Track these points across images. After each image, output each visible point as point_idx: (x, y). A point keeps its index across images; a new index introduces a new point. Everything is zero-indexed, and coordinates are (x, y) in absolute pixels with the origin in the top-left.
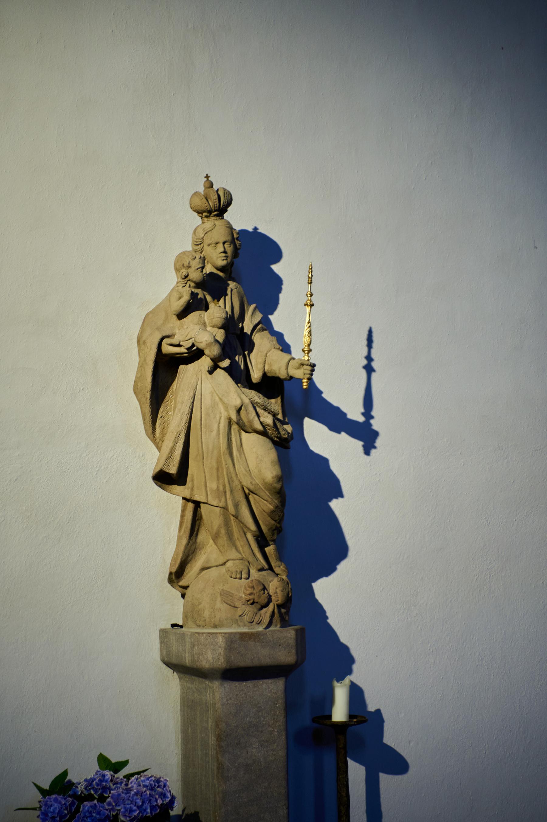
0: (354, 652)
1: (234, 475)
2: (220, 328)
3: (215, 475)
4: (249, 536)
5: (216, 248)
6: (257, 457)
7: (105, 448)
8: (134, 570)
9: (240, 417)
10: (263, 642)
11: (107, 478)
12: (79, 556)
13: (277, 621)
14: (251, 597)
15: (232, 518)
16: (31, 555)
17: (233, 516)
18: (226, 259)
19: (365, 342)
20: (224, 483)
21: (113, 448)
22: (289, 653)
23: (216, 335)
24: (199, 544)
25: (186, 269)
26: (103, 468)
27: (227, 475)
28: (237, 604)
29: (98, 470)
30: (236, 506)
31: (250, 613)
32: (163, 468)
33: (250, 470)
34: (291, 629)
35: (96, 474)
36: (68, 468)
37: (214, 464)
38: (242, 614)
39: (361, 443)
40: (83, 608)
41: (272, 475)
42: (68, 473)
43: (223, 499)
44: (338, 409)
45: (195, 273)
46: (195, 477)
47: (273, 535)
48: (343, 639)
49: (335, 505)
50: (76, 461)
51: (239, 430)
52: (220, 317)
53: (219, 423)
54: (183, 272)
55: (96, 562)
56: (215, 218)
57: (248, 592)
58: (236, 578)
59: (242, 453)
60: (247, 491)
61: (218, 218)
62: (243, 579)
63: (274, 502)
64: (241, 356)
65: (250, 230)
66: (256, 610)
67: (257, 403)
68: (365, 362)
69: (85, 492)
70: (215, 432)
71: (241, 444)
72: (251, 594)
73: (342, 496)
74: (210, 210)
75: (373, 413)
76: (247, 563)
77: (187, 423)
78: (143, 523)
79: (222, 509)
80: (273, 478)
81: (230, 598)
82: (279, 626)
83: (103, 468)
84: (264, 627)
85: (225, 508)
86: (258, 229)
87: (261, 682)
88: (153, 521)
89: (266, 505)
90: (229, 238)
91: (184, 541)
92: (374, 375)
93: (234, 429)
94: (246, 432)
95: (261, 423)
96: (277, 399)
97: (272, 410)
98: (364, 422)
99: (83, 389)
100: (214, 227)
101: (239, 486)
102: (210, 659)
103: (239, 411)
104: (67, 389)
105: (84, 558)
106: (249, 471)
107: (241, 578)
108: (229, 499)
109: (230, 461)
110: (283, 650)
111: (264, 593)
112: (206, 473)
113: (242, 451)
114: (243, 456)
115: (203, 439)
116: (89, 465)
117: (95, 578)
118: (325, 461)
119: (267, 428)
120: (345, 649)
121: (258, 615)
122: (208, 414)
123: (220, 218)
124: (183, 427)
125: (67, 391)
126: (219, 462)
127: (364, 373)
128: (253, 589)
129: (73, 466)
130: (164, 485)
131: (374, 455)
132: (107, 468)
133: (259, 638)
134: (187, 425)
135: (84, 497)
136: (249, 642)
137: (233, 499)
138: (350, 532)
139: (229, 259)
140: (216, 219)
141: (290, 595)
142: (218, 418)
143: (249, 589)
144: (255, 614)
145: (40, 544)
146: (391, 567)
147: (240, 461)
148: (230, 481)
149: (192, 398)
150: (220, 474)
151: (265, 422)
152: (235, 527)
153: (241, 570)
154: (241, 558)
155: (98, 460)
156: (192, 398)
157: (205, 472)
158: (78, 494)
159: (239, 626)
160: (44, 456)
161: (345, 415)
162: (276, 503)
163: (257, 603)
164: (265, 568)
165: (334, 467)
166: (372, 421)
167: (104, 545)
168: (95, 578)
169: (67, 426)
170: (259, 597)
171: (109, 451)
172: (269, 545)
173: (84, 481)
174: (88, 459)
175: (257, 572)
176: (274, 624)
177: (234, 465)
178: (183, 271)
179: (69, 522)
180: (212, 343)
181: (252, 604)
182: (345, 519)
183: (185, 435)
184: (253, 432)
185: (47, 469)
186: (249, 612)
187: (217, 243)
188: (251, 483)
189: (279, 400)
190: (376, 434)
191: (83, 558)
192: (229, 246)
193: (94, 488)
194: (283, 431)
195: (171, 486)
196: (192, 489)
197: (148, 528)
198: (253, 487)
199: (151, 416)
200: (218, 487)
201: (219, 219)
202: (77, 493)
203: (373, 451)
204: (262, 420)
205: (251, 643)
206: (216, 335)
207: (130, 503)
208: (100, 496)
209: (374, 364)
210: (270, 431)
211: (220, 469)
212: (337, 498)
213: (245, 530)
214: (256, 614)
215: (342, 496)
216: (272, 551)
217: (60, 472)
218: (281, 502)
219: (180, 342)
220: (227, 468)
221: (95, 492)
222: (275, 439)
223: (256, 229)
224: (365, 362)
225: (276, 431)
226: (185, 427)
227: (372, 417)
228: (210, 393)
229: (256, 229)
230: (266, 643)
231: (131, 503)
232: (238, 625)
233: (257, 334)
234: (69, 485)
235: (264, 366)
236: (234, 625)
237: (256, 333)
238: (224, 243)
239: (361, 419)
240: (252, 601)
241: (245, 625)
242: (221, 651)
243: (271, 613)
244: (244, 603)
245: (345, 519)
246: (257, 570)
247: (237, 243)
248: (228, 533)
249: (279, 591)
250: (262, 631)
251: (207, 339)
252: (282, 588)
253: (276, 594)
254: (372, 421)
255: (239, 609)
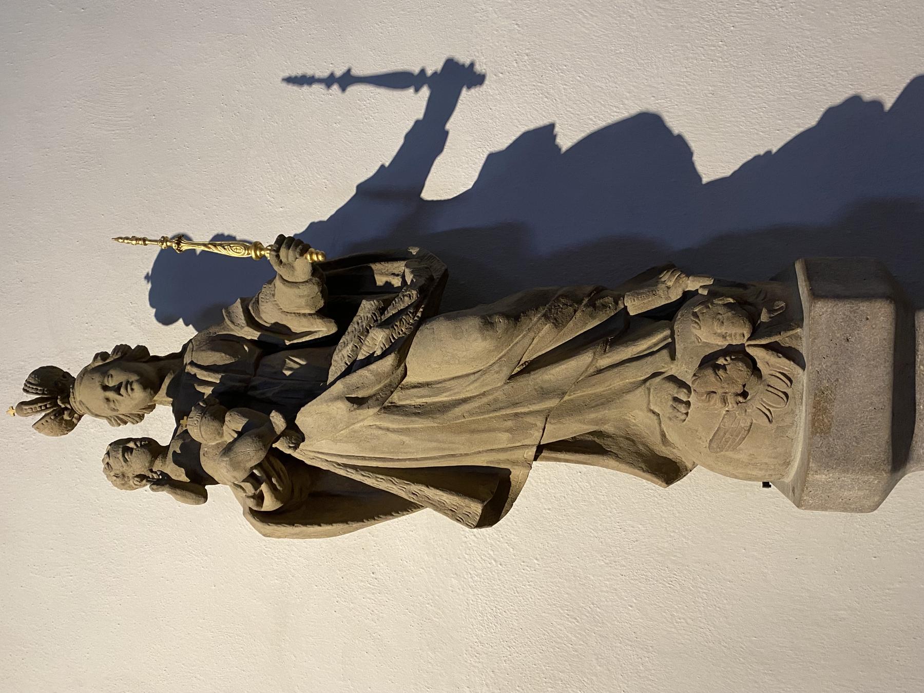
0: (838, 99)
1: (485, 400)
2: (222, 421)
3: (485, 436)
4: (604, 362)
5: (117, 400)
6: (448, 362)
7: (462, 546)
8: (661, 513)
9: (370, 397)
10: (837, 380)
11: (508, 547)
12: (631, 606)
13: (787, 335)
14: (731, 399)
15: (566, 398)
16: (626, 688)
17: (562, 398)
18: (131, 384)
19: (305, 88)
20: (498, 417)
21: (462, 533)
22: (868, 319)
23: (234, 430)
24: (619, 428)
25: (129, 481)
26: (491, 553)
27: (483, 413)
28: (744, 424)
29: (495, 561)
30: (544, 393)
31: (764, 399)
32: (472, 526)
33: (474, 373)
34: (810, 311)
35: (501, 564)
36: (490, 611)
37: (464, 437)
38: (766, 415)
39: (464, 91)
40: (719, 608)
41: (480, 340)
42: (498, 611)
43: (530, 419)
44: (407, 137)
45: (133, 465)
46: (492, 459)
47: (605, 306)
48: (812, 121)
49: (566, 140)
50: (480, 596)
51: (401, 388)
52: (199, 428)
53: (388, 429)
54: (135, 484)
55: (643, 578)
56: (71, 400)
57: (719, 405)
58: (687, 414)
59: (443, 385)
60: (518, 369)
61: (71, 394)
62: (689, 400)
63: (535, 325)
64: (287, 361)
65: (149, 286)
66: (761, 387)
67: (356, 349)
68: (335, 87)
69: (528, 587)
70: (405, 439)
71: (428, 384)
72: (724, 401)
73: (552, 126)
74: (55, 415)
75: (416, 70)
76: (658, 379)
77: (393, 481)
78: (581, 492)
79: (548, 419)
80: (485, 339)
81: (727, 435)
82: (799, 330)
83: (491, 553)
84: (800, 370)
85: (547, 415)
86: (148, 274)
87: (922, 367)
88: (579, 474)
89: (543, 337)
90: (97, 378)
91: (612, 462)
92: (356, 72)
93: (399, 400)
94: (405, 375)
95: (384, 355)
96: (375, 272)
97: (369, 316)
98: (430, 87)
99: (373, 573)
100: (83, 404)
101: (506, 387)
102: (861, 493)
103: (358, 402)
104: (373, 598)
105: (636, 599)
106: (476, 375)
107: (688, 404)
108: (529, 408)
109: (458, 411)
110: (858, 334)
111: (724, 367)
112: (481, 450)
113: (439, 385)
114: (448, 384)
115: (418, 456)
116: (486, 574)
117: (670, 583)
118: (492, 158)
119: (396, 338)
120: (831, 114)
121: (773, 382)
122: (373, 449)
123: (71, 390)
124: (400, 488)
125: (376, 600)
126: (459, 429)
127: (354, 90)
128: (714, 395)
129: (487, 602)
130: (511, 495)
131: (485, 67)
132: (492, 545)
133: (827, 388)
134: (395, 479)
135: (536, 589)
136: (833, 414)
137: (529, 401)
138: (615, 109)
139: (134, 378)
140: (74, 398)
141: (731, 300)
142: (380, 432)
143: (712, 402)
144: (770, 389)
145: (609, 670)
146: (682, 26)
147: (456, 391)
148: (494, 406)
149: (348, 471)
150: (482, 427)
151: (382, 346)
152: (585, 391)
153: (670, 398)
154: (647, 392)
155: (479, 558)
156: (348, 471)
157: (480, 452)
158: (531, 598)
159: (793, 424)
160: (471, 647)
161: (417, 122)
162: (540, 319)
163: (744, 386)
164: (670, 340)
165: (502, 142)
166: (429, 72)
167: (615, 562)
168: (670, 583)
169: (427, 606)
170: (732, 381)
171: (465, 539)
172: (626, 307)
173: (511, 586)
174: (477, 576)
175: (675, 362)
176: (793, 344)
177: (465, 401)
178: (133, 484)
179: (576, 619)
180: (231, 460)
181: (744, 394)
182: (591, 119)
183: (413, 483)
184: (403, 365)
185: (491, 644)
186: (764, 402)
187: (108, 400)
188: (497, 372)
189: (376, 267)
190: (450, 64)
191: (635, 601)
192: (110, 378)
193: (523, 571)
194: (403, 302)
195: (513, 483)
196: (514, 463)
197: (590, 484)
198: (505, 369)
199: (393, 514)
200: (507, 430)
201: (73, 392)
202: (530, 600)
203: (478, 68)
204: (379, 352)
205: (837, 409)
206: (234, 430)
207: (548, 511)
208: (536, 561)
209: (339, 73)
210: (402, 329)
211: (473, 426)
212: (554, 137)
213: (591, 370)
214: (769, 386)
215: (552, 126)
216: (636, 302)
217: (496, 624)
218: (537, 309)
219: (248, 497)
220: (471, 414)
221: (529, 570)
222: (419, 314)
223: (147, 277)
224: (335, 87)
225: (401, 320)
226: (400, 483)
227: (423, 71)
228: (336, 444)
229: (147, 277)
230: (838, 373)
231: (549, 509)
232: (789, 427)
233: (263, 316)
234: (516, 611)
235: (304, 315)
236: (790, 433)
237: (261, 318)
238: (105, 388)
239: (425, 92)
240: (741, 399)
241: (793, 412)
242: (847, 478)
243: (770, 352)
244: (744, 412)
245: (591, 119)
246: (673, 363)
247: (112, 359)
248: (597, 405)
249: (722, 330)
250: (808, 376)
251: (225, 470)
252: (716, 324)
253: (728, 338)
254: (429, 72)
255: (754, 421)
